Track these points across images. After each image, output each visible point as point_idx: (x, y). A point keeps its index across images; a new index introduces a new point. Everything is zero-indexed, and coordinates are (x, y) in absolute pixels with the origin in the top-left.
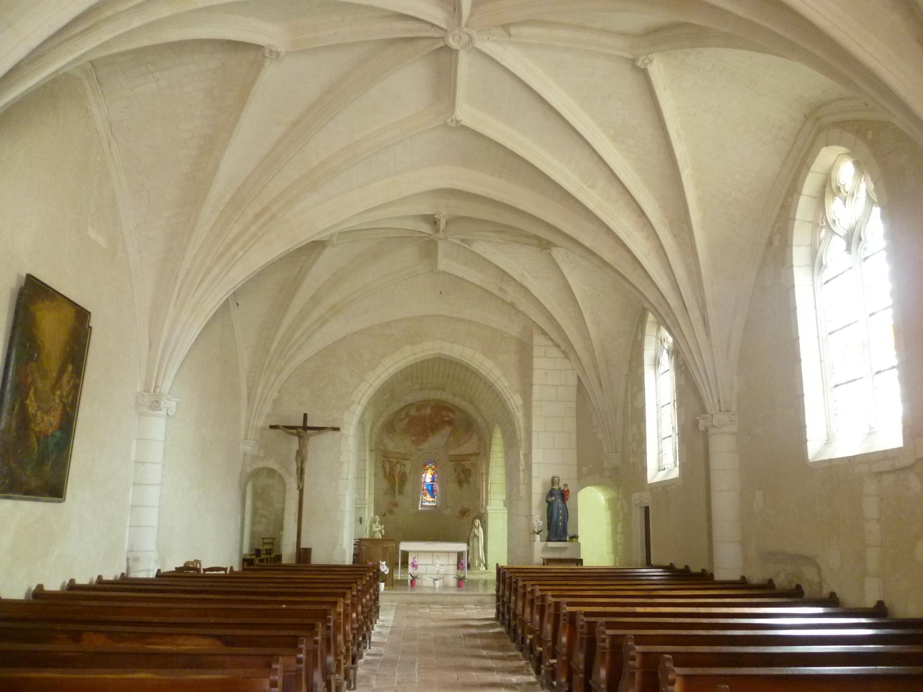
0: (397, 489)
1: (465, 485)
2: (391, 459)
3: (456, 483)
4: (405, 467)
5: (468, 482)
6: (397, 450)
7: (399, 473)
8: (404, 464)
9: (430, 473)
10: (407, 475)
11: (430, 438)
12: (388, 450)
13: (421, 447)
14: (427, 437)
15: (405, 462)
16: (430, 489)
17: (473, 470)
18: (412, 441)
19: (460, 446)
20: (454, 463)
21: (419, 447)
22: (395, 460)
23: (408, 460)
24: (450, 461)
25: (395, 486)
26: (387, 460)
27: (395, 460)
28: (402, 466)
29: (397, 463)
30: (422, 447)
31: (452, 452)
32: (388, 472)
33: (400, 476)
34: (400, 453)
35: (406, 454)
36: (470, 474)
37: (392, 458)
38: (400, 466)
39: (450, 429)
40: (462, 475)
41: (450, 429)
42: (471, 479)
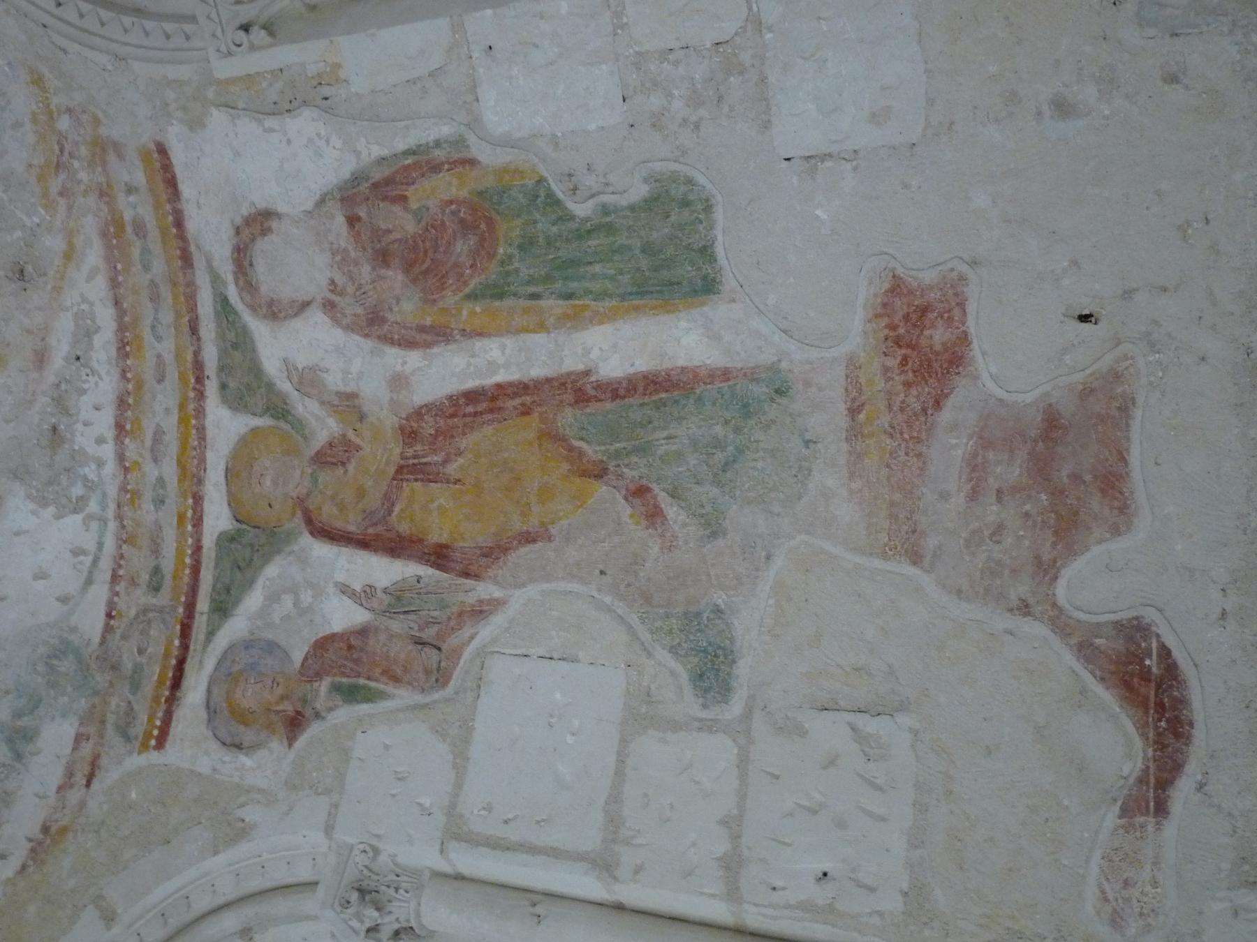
2: (217, 518)
12: (91, 622)
26: (222, 609)
28: (268, 282)
34: (126, 346)
38: (274, 312)
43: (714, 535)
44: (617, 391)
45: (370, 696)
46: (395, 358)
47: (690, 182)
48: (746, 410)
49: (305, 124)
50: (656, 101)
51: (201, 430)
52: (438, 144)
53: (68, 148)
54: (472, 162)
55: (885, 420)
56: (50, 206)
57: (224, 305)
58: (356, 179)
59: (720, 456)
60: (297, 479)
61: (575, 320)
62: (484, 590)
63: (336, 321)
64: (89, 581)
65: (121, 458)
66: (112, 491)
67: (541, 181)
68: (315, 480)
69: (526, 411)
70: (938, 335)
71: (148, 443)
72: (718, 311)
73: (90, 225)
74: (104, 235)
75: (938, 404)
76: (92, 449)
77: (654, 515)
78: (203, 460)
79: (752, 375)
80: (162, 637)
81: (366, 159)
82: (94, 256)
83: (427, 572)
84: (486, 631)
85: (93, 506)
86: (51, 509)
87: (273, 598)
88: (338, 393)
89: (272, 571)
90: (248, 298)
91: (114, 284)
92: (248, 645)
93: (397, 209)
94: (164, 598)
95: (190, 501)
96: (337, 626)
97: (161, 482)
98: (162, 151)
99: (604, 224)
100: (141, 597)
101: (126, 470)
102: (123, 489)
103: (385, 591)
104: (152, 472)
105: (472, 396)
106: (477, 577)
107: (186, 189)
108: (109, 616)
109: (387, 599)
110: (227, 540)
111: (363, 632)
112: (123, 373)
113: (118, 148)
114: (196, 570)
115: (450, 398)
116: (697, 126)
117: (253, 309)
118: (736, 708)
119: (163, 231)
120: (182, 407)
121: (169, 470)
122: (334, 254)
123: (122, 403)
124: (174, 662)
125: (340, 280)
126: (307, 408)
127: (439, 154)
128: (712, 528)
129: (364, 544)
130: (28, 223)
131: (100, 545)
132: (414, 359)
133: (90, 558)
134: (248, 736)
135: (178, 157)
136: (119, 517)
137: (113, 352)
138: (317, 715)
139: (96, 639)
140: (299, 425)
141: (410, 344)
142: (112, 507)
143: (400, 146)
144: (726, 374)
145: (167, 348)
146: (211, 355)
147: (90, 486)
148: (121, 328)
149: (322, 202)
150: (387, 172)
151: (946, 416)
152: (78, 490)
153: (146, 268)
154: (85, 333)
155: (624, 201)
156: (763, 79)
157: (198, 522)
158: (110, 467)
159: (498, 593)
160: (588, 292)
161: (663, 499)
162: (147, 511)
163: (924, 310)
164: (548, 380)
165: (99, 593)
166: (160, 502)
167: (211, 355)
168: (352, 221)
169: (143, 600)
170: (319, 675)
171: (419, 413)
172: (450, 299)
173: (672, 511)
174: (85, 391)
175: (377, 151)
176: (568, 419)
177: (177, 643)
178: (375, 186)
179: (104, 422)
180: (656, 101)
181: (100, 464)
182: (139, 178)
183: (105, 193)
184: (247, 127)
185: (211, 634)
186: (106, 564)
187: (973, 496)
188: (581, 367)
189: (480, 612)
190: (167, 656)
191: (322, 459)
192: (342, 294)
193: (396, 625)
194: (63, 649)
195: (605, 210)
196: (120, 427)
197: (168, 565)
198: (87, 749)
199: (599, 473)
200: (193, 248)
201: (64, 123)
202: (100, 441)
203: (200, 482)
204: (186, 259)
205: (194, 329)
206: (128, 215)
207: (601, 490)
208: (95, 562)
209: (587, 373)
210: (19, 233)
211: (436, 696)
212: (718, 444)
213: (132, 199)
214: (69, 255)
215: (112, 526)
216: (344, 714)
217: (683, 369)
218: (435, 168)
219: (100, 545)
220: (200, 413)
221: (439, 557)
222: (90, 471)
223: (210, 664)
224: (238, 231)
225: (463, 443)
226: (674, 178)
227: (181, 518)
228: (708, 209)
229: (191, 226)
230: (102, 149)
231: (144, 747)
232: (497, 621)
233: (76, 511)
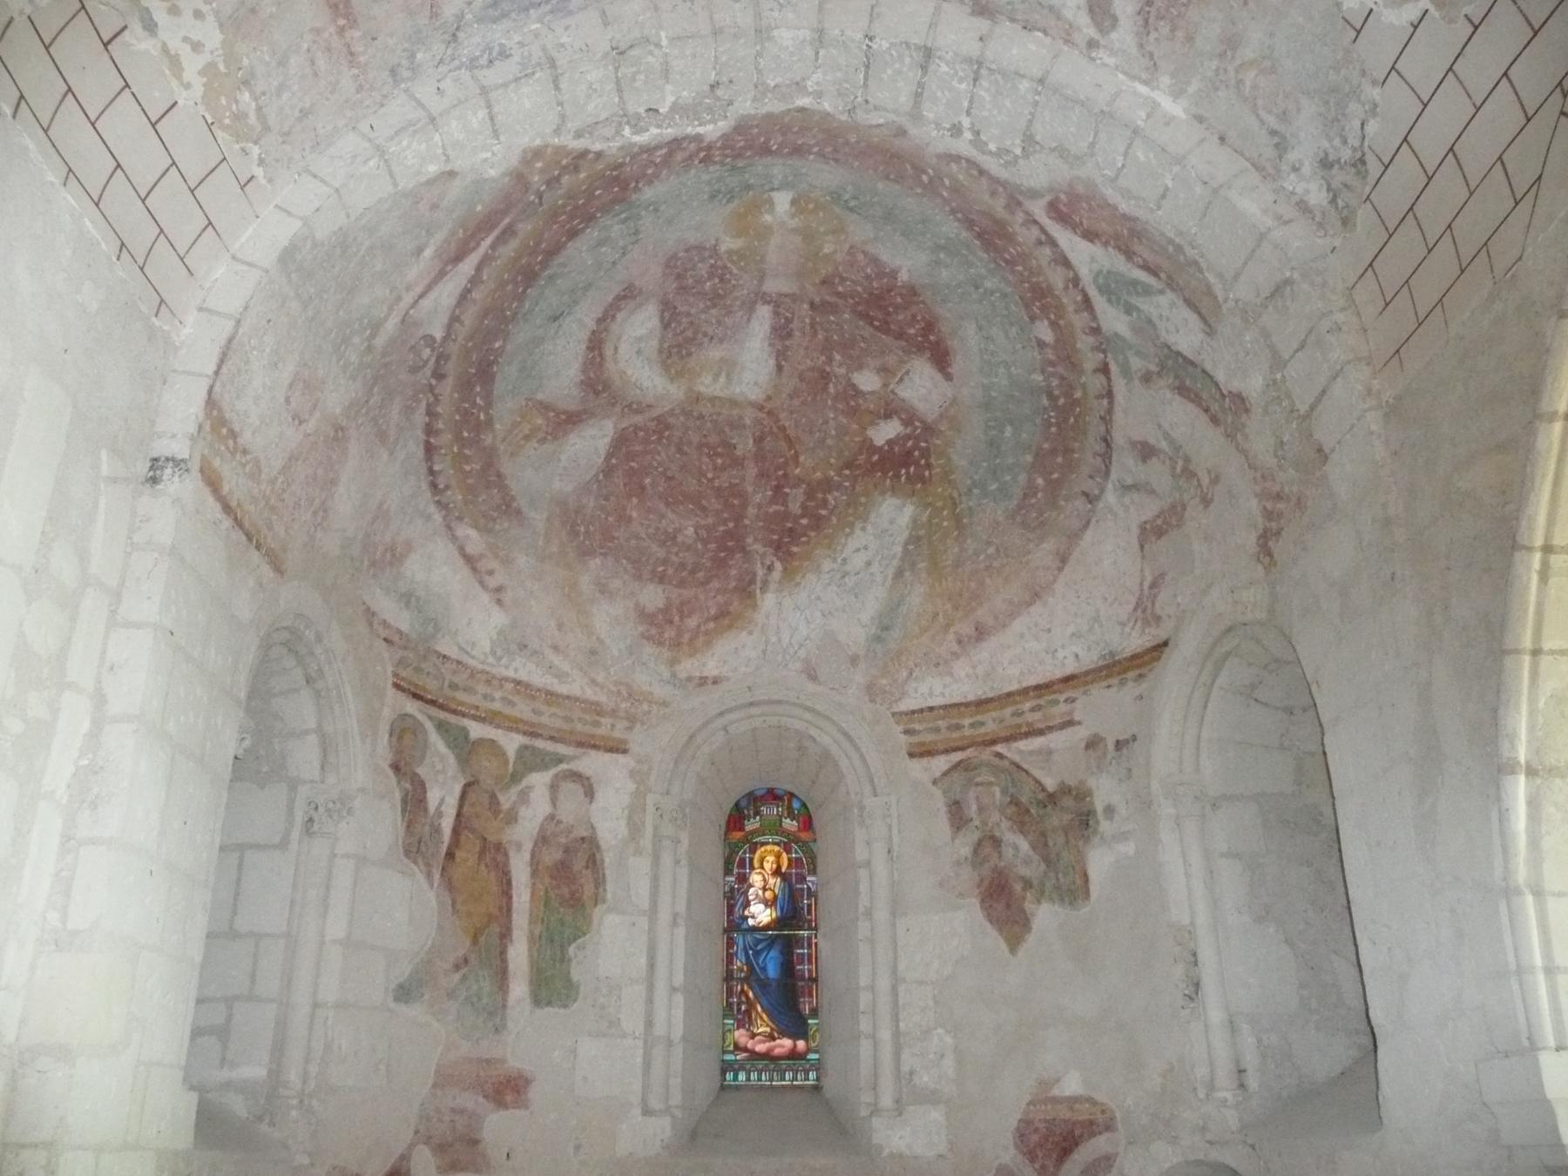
0: (519, 954)
1: (1046, 916)
2: (476, 730)
3: (974, 903)
4: (590, 793)
5: (1075, 891)
6: (523, 669)
7: (543, 840)
8: (576, 776)
9: (769, 864)
10: (608, 858)
11: (768, 601)
12: (445, 646)
13: (711, 665)
14: (746, 590)
15: (592, 763)
16: (773, 971)
17: (1105, 790)
18: (644, 616)
19: (981, 633)
20: (941, 763)
21: (688, 667)
22: (511, 743)
23: (618, 748)
24: (921, 752)
25: (506, 935)
26: (441, 727)
27: (511, 743)
28: (569, 787)
29: (531, 761)
30: (711, 667)
31: (930, 690)
32: (447, 825)
33: (551, 856)
34: (551, 697)
35: (597, 709)
36: (1084, 821)
38: (554, 788)
39: (909, 510)
40: (1018, 845)
41: (909, 510)
42: (1100, 862)
43: (448, 994)
44: (503, 953)
45: (404, 811)
46: (528, 846)
47: (575, 1000)
48: (491, 1014)
49: (623, 829)
50: (604, 991)
51: (510, 729)
52: (605, 890)
53: (637, 704)
54: (596, 905)
55: (482, 1073)
56: (616, 683)
57: (560, 760)
58: (598, 847)
59: (475, 1000)
60: (487, 782)
61: (532, 940)
62: (437, 876)
63: (546, 819)
64: (461, 648)
65: (506, 679)
66: (494, 671)
67: (584, 934)
68: (487, 792)
69: (500, 909)
70: (509, 1098)
71: (510, 697)
72: (527, 1004)
73: (603, 698)
74: (597, 704)
75: (485, 1097)
76: (514, 664)
77: (457, 967)
78: (498, 727)
79: (503, 1018)
80: (431, 686)
81: (605, 854)
82: (590, 694)
83: (444, 848)
84: (421, 878)
85: (491, 660)
86: (495, 637)
87: (442, 758)
88: (517, 813)
89: (451, 759)
90: (561, 775)
91: (577, 699)
92: (426, 741)
93: (584, 864)
94: (447, 691)
95: (483, 715)
96: (429, 794)
97: (493, 700)
98: (625, 751)
99: (564, 960)
100: (448, 677)
101: (501, 680)
102: (494, 677)
103: (439, 824)
104: (498, 695)
105: (509, 883)
106: (442, 875)
107: (608, 756)
108: (444, 657)
109: (436, 824)
110: (464, 731)
111: (426, 810)
112: (539, 690)
113: (630, 729)
114: (455, 712)
115: (510, 872)
116: (593, 1006)
117: (556, 776)
118: (392, 1005)
119: (593, 736)
120: (521, 720)
121: (497, 706)
122: (572, 826)
123: (528, 686)
124: (422, 694)
125: (562, 826)
127: (601, 890)
128: (451, 995)
129: (459, 815)
130: (612, 669)
131: (473, 657)
132: (527, 856)
133: (469, 650)
134: (394, 739)
135: (620, 758)
136: (483, 672)
137: (549, 688)
138: (399, 782)
139: (438, 648)
140: (507, 787)
141: (533, 855)
142: (488, 669)
143: (607, 872)
144: (504, 1006)
145: (544, 719)
146: (540, 744)
147: (500, 659)
148: (558, 696)
149: (593, 827)
150: (598, 863)
151: (481, 1099)
152: (499, 652)
153: (580, 719)
154: (561, 676)
155: (572, 971)
156: (604, 1035)
157: (475, 718)
159: (436, 885)
160: (541, 946)
161: (464, 970)
162: (482, 689)
163: (518, 1092)
164: (510, 922)
165: (453, 652)
166: (485, 697)
167: (540, 744)
168: (583, 839)
169: (447, 677)
170: (412, 783)
171: (506, 855)
172: (547, 880)
173: (457, 977)
174: (537, 666)
175: (607, 860)
176: (496, 929)
177: (429, 697)
178: (594, 855)
179: (522, 675)
180: (604, 991)
181: (507, 667)
182: (617, 734)
183: (614, 713)
184: (626, 800)
185: (430, 718)
186: (465, 659)
187: (453, 1110)
188: (514, 938)
189: (429, 875)
190: (425, 689)
191: (493, 796)
192: (556, 825)
193: (427, 828)
194: (437, 629)
195: (570, 960)
196: (518, 683)
197: (461, 696)
198: (396, 639)
199: (475, 941)
200: (583, 750)
201: (645, 707)
202: (516, 670)
203: (491, 723)
204: (580, 744)
205: (552, 738)
206: (603, 720)
207: (468, 943)
208: (467, 653)
209: (511, 941)
210: (610, 662)
211: (401, 850)
212: (480, 999)
213: (609, 726)
214: (593, 682)
215: (480, 667)
216: (398, 796)
217: (508, 987)
218: (597, 887)
219: (473, 657)
220: (517, 731)
221: (450, 855)
222: (504, 661)
223: (420, 717)
224: (588, 779)
225: (493, 874)
226: (578, 993)
227: (477, 708)
228: (565, 1006)
229: (593, 753)
230: (632, 720)
231: (396, 675)
232: (425, 886)
233: (492, 649)
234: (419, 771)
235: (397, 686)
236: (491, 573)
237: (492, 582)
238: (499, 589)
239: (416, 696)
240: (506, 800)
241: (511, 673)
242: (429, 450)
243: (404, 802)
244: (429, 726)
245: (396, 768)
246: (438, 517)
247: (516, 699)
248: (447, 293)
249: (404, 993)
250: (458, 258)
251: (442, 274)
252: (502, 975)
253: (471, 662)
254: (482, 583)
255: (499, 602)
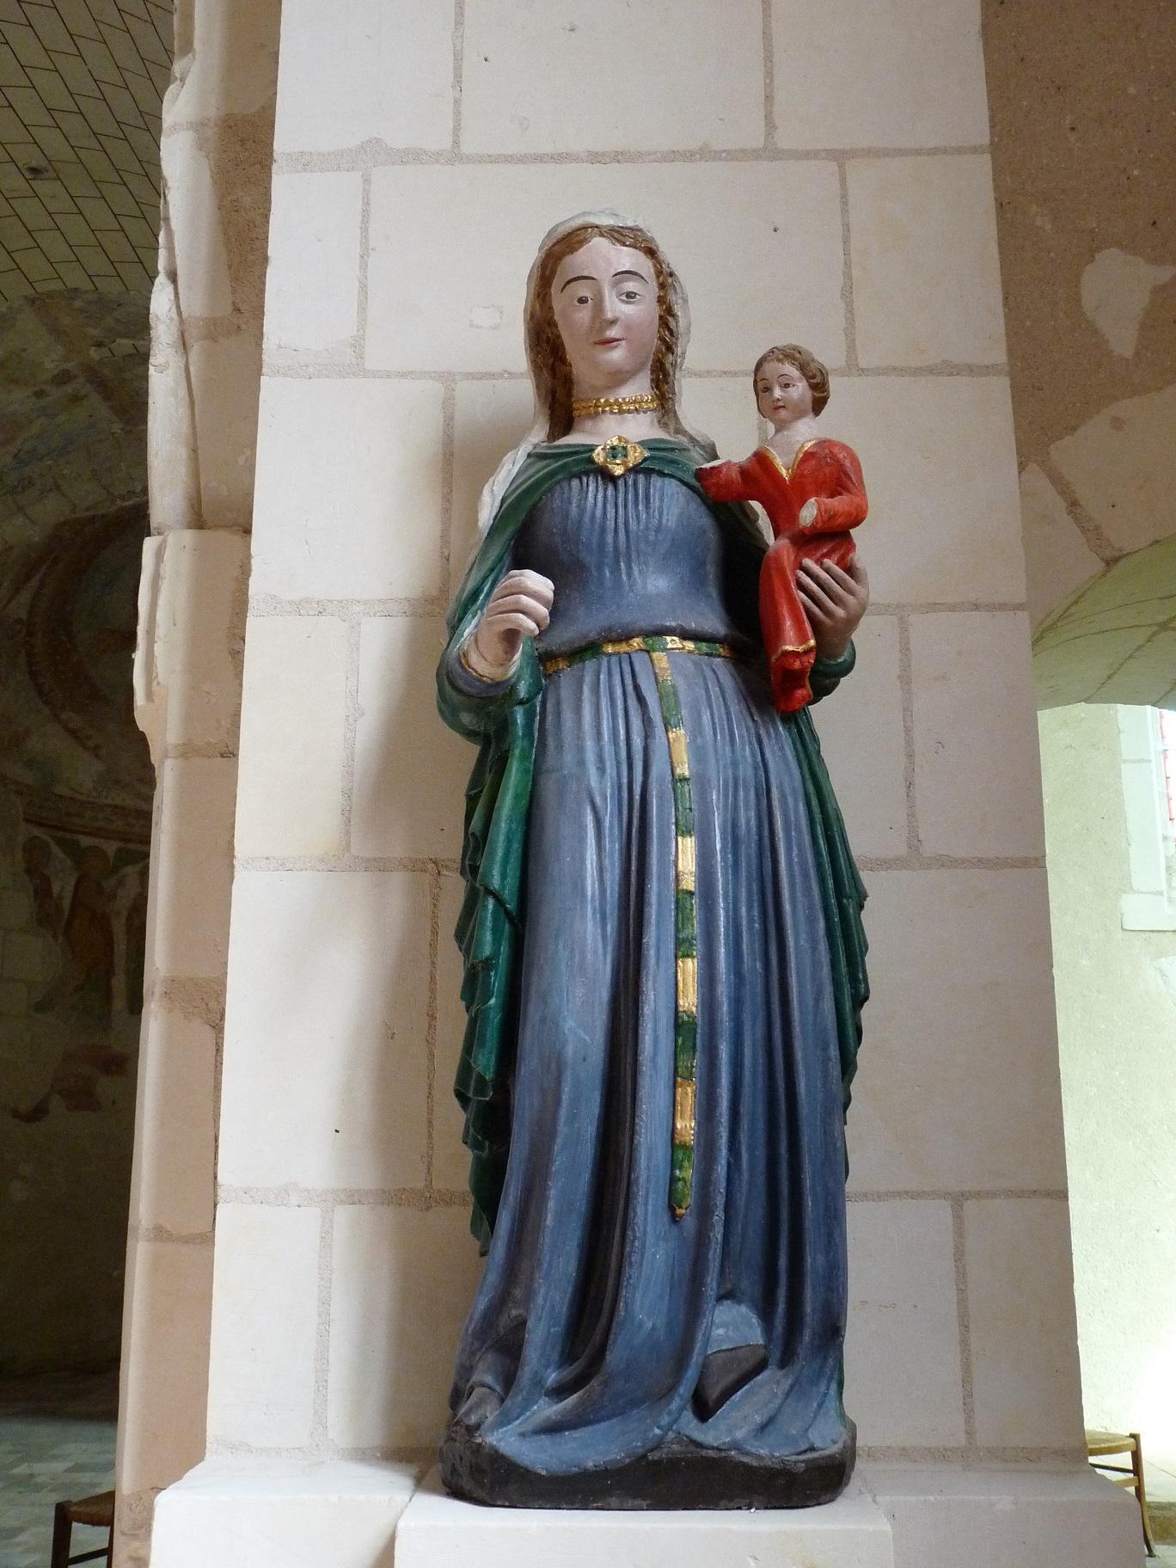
2: (85, 841)
12: (61, 789)
22: (111, 847)
25: (110, 972)
26: (60, 842)
27: (111, 847)
32: (67, 903)
37: (97, 833)
46: (125, 913)
51: (111, 838)
62: (61, 938)
64: (72, 789)
65: (106, 805)
85: (94, 794)
89: (69, 863)
111: (52, 897)
123: (123, 808)
126: (113, 881)
131: (82, 794)
132: (123, 920)
136: (90, 802)
139: (56, 791)
146: (132, 846)
157: (83, 833)
158: (105, 801)
167: (132, 846)
179: (118, 801)
181: (107, 798)
185: (53, 838)
186: (76, 796)
189: (55, 936)
196: (116, 807)
215: (85, 799)
219: (82, 794)
221: (70, 923)
223: (44, 837)
231: (24, 813)
233: (94, 788)
234: (46, 872)
235: (27, 821)
236: (89, 738)
237: (90, 743)
238: (97, 747)
239: (40, 825)
240: (109, 884)
241: (109, 801)
242: (33, 675)
243: (36, 892)
244: (52, 843)
245: (28, 871)
246: (47, 711)
247: (113, 818)
248: (25, 597)
249: (41, 1007)
250: (28, 577)
251: (17, 590)
252: (108, 997)
253: (80, 797)
254: (84, 746)
255: (97, 756)
